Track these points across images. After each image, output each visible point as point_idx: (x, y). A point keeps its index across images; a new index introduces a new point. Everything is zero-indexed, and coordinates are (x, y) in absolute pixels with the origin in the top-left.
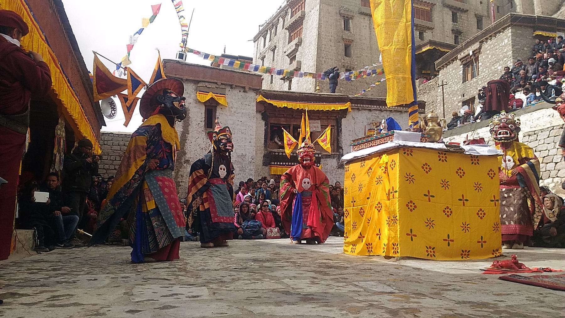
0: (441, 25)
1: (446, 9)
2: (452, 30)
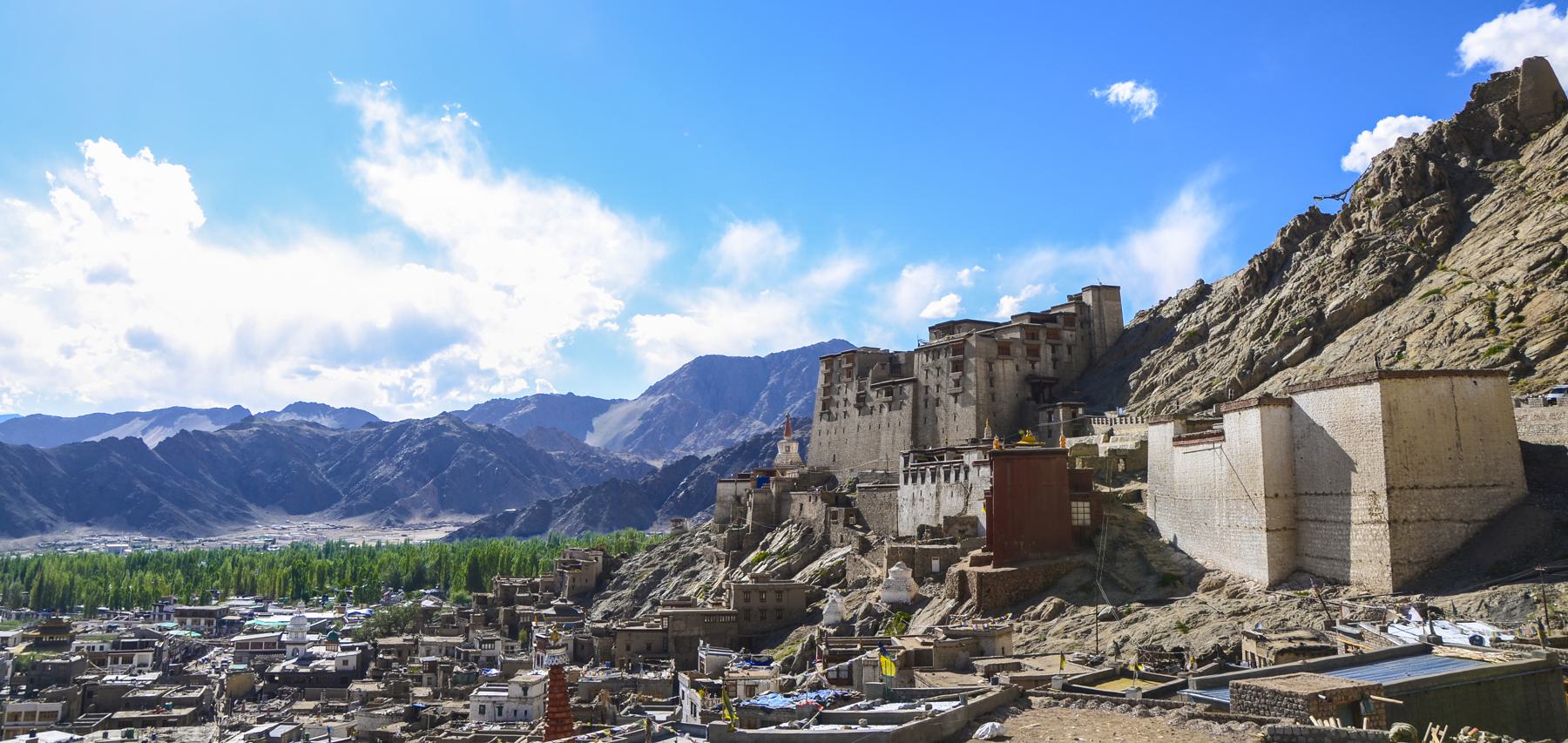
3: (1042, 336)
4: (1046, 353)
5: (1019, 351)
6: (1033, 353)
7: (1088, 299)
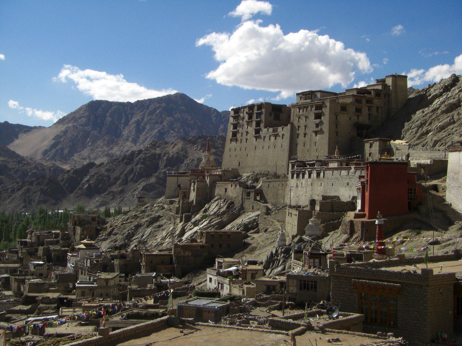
2: (368, 114)
3: (364, 101)
4: (365, 110)
5: (352, 109)
7: (389, 82)
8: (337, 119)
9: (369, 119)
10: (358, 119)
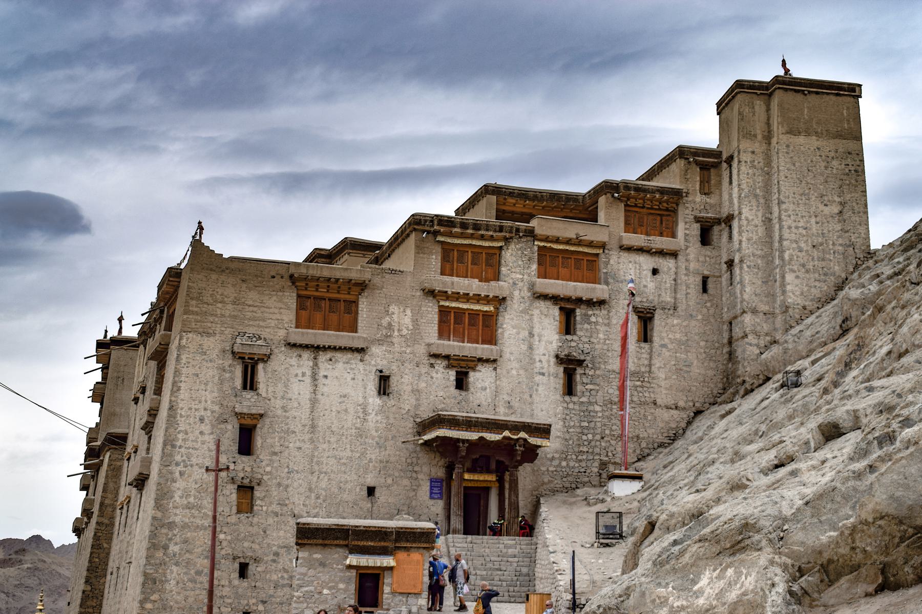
0: (524, 347)
1: (542, 305)
2: (557, 356)
3: (518, 269)
4: (529, 336)
6: (471, 324)
8: (249, 383)
9: (569, 389)
10: (461, 383)
